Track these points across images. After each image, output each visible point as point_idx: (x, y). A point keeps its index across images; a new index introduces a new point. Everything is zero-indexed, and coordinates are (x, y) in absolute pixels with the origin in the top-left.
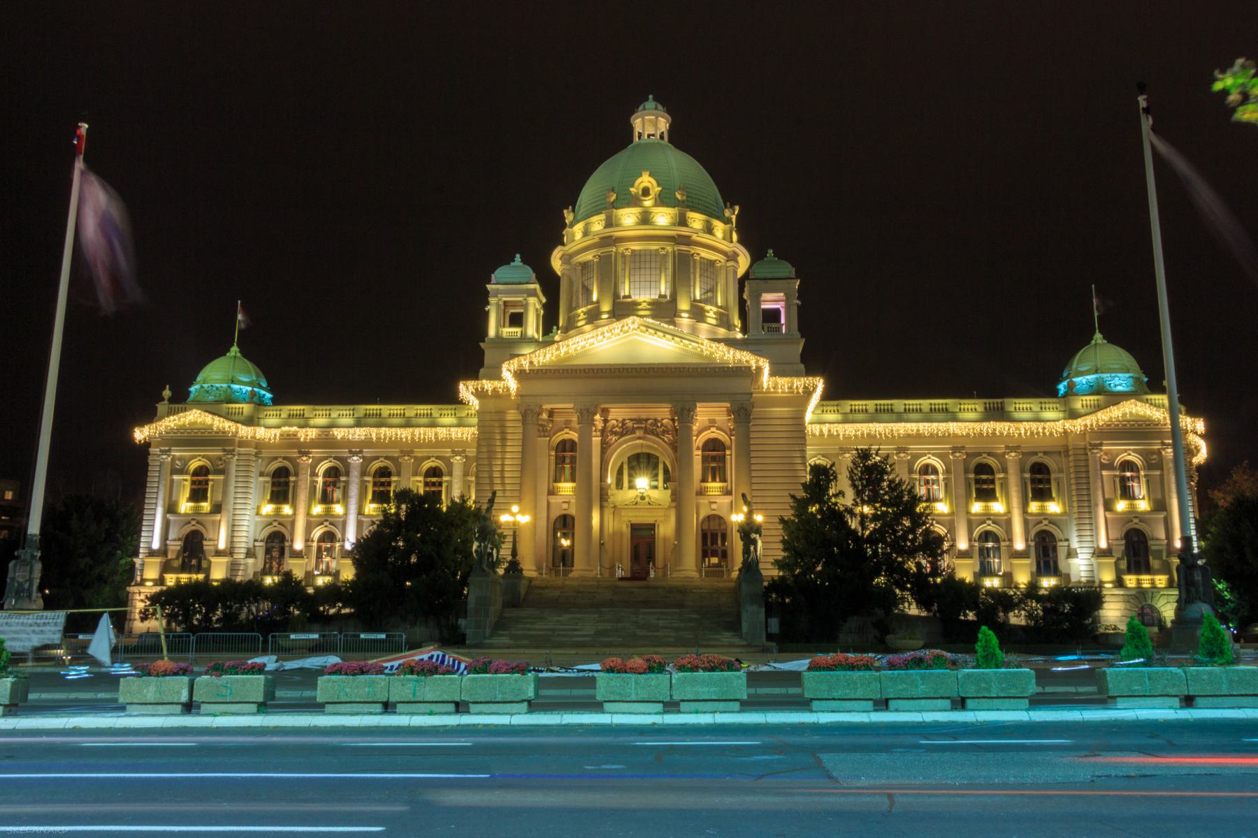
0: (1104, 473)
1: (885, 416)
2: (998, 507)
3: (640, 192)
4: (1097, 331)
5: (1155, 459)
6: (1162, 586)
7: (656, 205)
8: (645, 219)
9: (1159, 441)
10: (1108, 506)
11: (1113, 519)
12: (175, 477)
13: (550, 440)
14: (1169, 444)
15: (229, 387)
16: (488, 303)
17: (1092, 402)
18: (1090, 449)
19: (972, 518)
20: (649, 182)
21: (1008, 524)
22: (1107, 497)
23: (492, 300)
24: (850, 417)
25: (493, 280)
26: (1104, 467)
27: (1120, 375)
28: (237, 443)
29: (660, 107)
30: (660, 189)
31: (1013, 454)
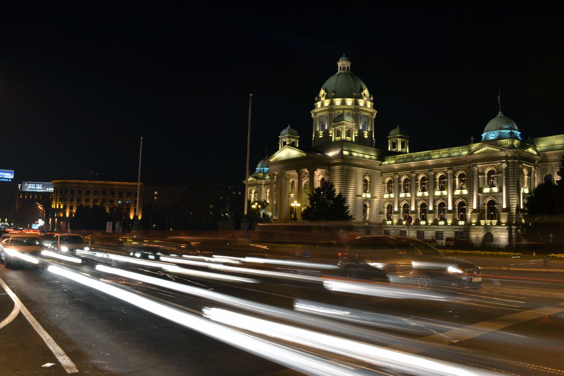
0: (480, 176)
1: (409, 160)
2: (445, 193)
3: (322, 96)
4: (500, 111)
6: (495, 225)
7: (325, 99)
8: (322, 105)
9: (499, 161)
10: (480, 190)
11: (482, 196)
12: (251, 195)
14: (504, 162)
15: (261, 169)
16: (279, 142)
17: (477, 146)
18: (472, 167)
19: (435, 197)
22: (480, 187)
23: (280, 141)
24: (398, 161)
27: (494, 132)
28: (259, 185)
29: (344, 59)
30: (326, 93)
31: (450, 171)
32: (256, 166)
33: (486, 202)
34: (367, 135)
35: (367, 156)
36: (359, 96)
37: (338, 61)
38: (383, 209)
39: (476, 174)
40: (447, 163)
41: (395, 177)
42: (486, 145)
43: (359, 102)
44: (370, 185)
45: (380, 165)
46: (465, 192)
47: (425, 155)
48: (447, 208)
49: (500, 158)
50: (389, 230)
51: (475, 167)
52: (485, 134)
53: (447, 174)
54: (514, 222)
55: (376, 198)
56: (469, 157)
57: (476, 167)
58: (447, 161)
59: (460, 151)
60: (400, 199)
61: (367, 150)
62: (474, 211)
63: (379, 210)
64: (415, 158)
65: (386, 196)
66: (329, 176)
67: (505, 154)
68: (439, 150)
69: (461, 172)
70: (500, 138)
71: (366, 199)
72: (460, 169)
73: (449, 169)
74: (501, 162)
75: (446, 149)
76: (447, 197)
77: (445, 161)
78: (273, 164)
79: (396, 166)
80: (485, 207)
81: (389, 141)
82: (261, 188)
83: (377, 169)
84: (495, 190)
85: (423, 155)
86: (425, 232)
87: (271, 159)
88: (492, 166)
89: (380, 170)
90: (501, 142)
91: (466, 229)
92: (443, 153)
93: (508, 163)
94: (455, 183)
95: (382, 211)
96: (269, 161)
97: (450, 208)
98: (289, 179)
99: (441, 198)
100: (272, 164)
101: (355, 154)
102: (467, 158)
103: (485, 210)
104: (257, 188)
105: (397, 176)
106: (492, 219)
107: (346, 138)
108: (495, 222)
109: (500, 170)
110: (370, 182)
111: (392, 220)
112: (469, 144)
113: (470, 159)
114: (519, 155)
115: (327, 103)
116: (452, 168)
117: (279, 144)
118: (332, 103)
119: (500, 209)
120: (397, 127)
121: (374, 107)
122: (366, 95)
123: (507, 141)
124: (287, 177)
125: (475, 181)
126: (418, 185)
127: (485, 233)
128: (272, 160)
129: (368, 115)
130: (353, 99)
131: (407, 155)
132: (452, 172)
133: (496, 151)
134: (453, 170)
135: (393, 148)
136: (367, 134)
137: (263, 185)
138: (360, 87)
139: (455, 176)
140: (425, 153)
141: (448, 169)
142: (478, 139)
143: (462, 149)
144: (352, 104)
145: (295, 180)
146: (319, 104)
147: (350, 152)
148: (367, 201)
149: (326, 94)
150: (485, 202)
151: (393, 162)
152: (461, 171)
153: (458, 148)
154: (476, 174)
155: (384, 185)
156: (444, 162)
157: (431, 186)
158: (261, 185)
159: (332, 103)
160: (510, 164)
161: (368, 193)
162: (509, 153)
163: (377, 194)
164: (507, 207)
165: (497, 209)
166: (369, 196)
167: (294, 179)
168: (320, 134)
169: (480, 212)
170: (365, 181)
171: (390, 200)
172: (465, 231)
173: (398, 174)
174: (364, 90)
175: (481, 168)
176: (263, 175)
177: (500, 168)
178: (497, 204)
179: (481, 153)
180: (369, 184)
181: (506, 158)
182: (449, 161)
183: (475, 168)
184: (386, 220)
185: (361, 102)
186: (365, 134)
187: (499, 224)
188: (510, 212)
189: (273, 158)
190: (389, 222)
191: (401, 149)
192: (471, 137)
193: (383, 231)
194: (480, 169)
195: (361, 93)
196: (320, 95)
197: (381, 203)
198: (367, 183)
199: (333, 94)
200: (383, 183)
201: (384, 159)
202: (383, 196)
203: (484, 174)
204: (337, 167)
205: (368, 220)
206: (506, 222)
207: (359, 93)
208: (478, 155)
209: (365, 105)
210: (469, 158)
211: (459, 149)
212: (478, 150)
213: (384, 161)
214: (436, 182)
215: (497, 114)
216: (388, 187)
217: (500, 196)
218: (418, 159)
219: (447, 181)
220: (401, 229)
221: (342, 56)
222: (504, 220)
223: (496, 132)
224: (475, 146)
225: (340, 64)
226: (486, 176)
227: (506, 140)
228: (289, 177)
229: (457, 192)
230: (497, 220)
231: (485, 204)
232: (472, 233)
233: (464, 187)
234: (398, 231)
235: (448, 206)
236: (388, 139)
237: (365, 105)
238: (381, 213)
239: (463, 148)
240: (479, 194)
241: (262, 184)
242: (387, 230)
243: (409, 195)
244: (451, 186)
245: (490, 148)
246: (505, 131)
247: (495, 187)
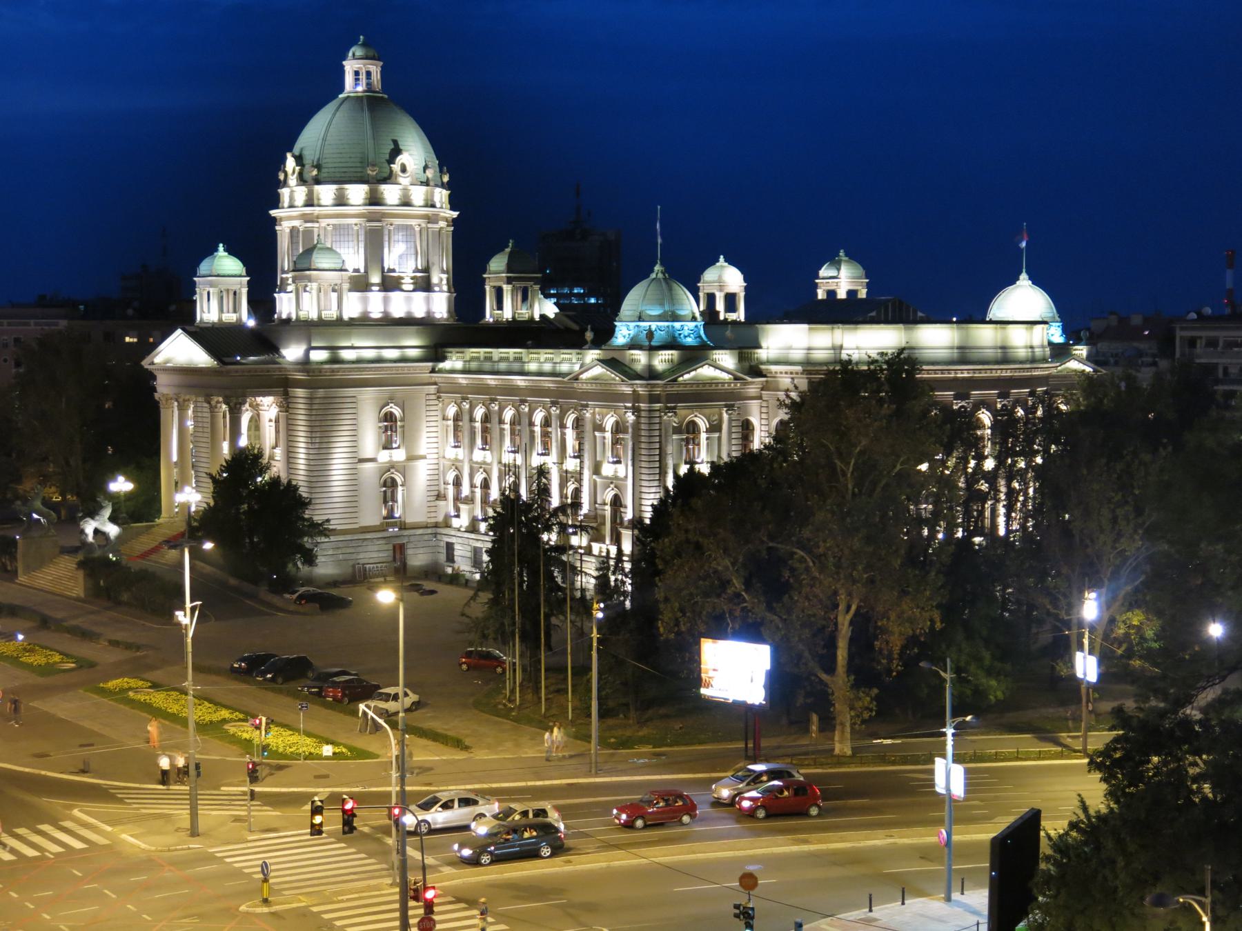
16: (195, 293)
22: (598, 459)
36: (386, 175)
38: (446, 486)
43: (385, 192)
44: (403, 427)
49: (621, 397)
55: (424, 457)
63: (436, 488)
65: (451, 453)
66: (287, 411)
71: (392, 466)
80: (605, 510)
81: (487, 288)
83: (426, 381)
89: (435, 384)
93: (636, 410)
95: (443, 492)
101: (347, 355)
103: (604, 517)
110: (402, 420)
117: (196, 300)
122: (408, 168)
138: (392, 147)
143: (577, 356)
155: (445, 422)
166: (399, 455)
170: (389, 417)
180: (399, 423)
181: (636, 397)
184: (452, 517)
185: (391, 193)
186: (403, 281)
193: (443, 544)
195: (392, 165)
197: (436, 476)
198: (396, 421)
199: (315, 172)
200: (444, 419)
201: (445, 352)
205: (400, 517)
207: (386, 165)
213: (443, 359)
231: (605, 504)
234: (469, 548)
236: (483, 281)
238: (440, 496)
240: (594, 477)
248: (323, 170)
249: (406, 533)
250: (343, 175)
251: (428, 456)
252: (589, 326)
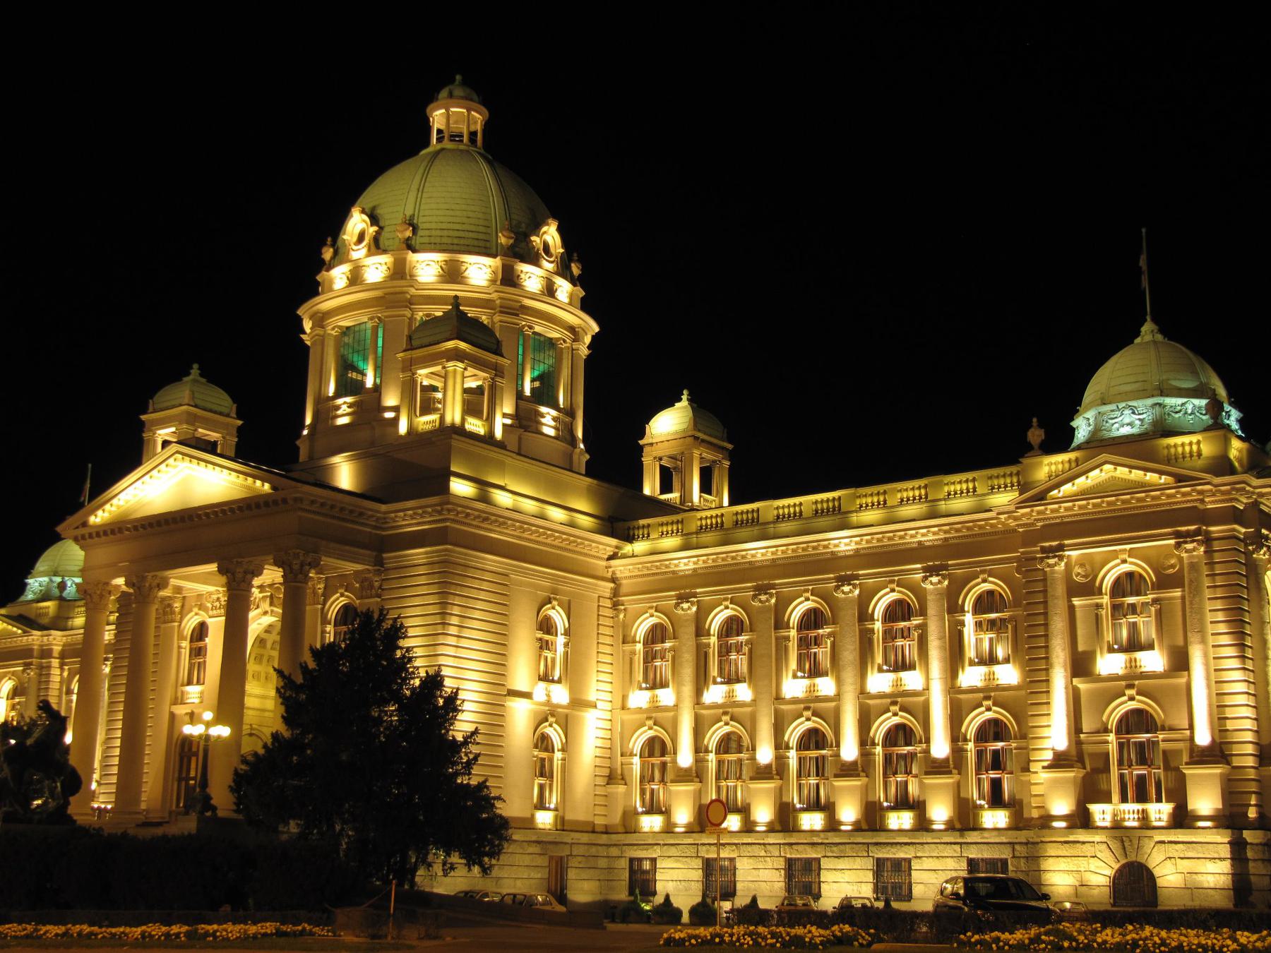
0: (1077, 602)
1: (744, 532)
2: (912, 680)
3: (355, 239)
4: (1148, 318)
5: (1173, 566)
7: (370, 253)
8: (355, 279)
10: (1081, 666)
11: (1092, 693)
13: (180, 625)
14: (1188, 534)
15: (51, 580)
18: (1042, 559)
19: (870, 702)
20: (364, 221)
21: (924, 716)
22: (1081, 648)
24: (694, 539)
25: (151, 409)
26: (1075, 589)
27: (1131, 403)
28: (35, 654)
29: (458, 92)
31: (935, 579)
32: (27, 568)
33: (1113, 722)
34: (553, 424)
35: (557, 514)
37: (429, 97)
38: (625, 760)
39: (1059, 590)
40: (920, 543)
41: (680, 612)
42: (1104, 457)
43: (522, 276)
45: (613, 557)
46: (1009, 675)
47: (816, 511)
48: (927, 752)
50: (654, 860)
51: (1056, 559)
52: (1091, 414)
53: (921, 595)
54: (1252, 813)
56: (1023, 515)
57: (1061, 558)
58: (923, 535)
59: (979, 491)
60: (704, 712)
61: (556, 487)
62: (1060, 762)
64: (774, 522)
65: (639, 699)
67: (1195, 496)
68: (881, 488)
69: (986, 587)
70: (1162, 428)
72: (983, 572)
73: (930, 571)
74: (1177, 535)
75: (916, 483)
76: (922, 698)
77: (912, 536)
78: (104, 538)
79: (686, 562)
80: (1108, 742)
82: (44, 671)
84: (1153, 661)
85: (806, 510)
86: (825, 863)
87: (93, 511)
88: (1131, 553)
90: (1168, 447)
91: (1017, 847)
92: (902, 500)
93: (1208, 540)
94: (960, 634)
95: (619, 772)
96: (85, 524)
97: (940, 748)
98: (183, 613)
99: (894, 703)
100: (98, 535)
101: (502, 498)
102: (1016, 519)
103: (1106, 755)
104: (24, 671)
105: (689, 609)
106: (1142, 797)
107: (463, 420)
108: (1160, 811)
109: (1171, 571)
111: (666, 812)
112: (1023, 456)
113: (1032, 524)
114: (1256, 504)
115: (376, 269)
116: (946, 567)
118: (400, 272)
119: (1178, 752)
120: (680, 400)
121: (587, 305)
122: (552, 250)
123: (1198, 443)
124: (170, 606)
125: (1058, 625)
126: (786, 648)
127: (1117, 866)
128: (99, 517)
129: (558, 339)
130: (499, 258)
131: (737, 514)
132: (946, 583)
133: (1150, 485)
134: (949, 574)
135: (662, 492)
136: (555, 419)
137: (56, 654)
139: (960, 602)
140: (816, 502)
141: (925, 570)
142: (1060, 440)
143: (990, 483)
144: (493, 281)
145: (210, 621)
146: (338, 276)
147: (482, 484)
148: (551, 719)
149: (373, 229)
150: (1104, 718)
151: (671, 542)
152: (984, 581)
153: (970, 475)
154: (1059, 590)
155: (627, 647)
156: (908, 540)
157: (849, 654)
158: (46, 653)
159: (400, 272)
160: (1215, 543)
161: (559, 681)
162: (1214, 495)
163: (598, 687)
164: (1213, 740)
165: (1164, 752)
167: (207, 612)
168: (338, 408)
169: (1084, 768)
171: (659, 715)
172: (1014, 857)
173: (695, 595)
174: (545, 229)
175: (1082, 565)
176: (60, 607)
177: (1173, 561)
178: (1163, 729)
179: (1085, 494)
182: (931, 537)
183: (1055, 564)
184: (637, 814)
185: (532, 277)
186: (543, 420)
187: (1183, 818)
188: (1228, 763)
189: (107, 507)
190: (650, 823)
191: (700, 497)
192: (1030, 426)
193: (624, 864)
194: (1077, 570)
195: (533, 238)
196: (345, 237)
199: (409, 233)
201: (629, 529)
202: (624, 698)
203: (1100, 592)
204: (418, 554)
206: (1217, 810)
208: (1070, 504)
209: (550, 291)
210: (1025, 520)
211: (974, 480)
212: (1071, 479)
213: (630, 539)
214: (872, 631)
215: (1137, 334)
216: (649, 657)
217: (1175, 689)
218: (784, 527)
219: (923, 628)
220: (708, 851)
221: (452, 81)
222: (1205, 801)
223: (1143, 404)
224: (1049, 465)
225: (438, 118)
226: (1106, 600)
227: (1194, 438)
228: (183, 606)
229: (971, 677)
230: (1168, 801)
231: (1106, 730)
232: (1048, 864)
233: (1000, 652)
235: (928, 741)
237: (550, 291)
239: (990, 478)
240: (1075, 681)
241: (50, 651)
242: (640, 860)
243: (743, 692)
244: (942, 648)
245: (1122, 472)
246: (1180, 401)
247: (1150, 647)
248: (420, 233)
249: (569, 838)
250: (456, 241)
251: (599, 704)
252: (1035, 420)
